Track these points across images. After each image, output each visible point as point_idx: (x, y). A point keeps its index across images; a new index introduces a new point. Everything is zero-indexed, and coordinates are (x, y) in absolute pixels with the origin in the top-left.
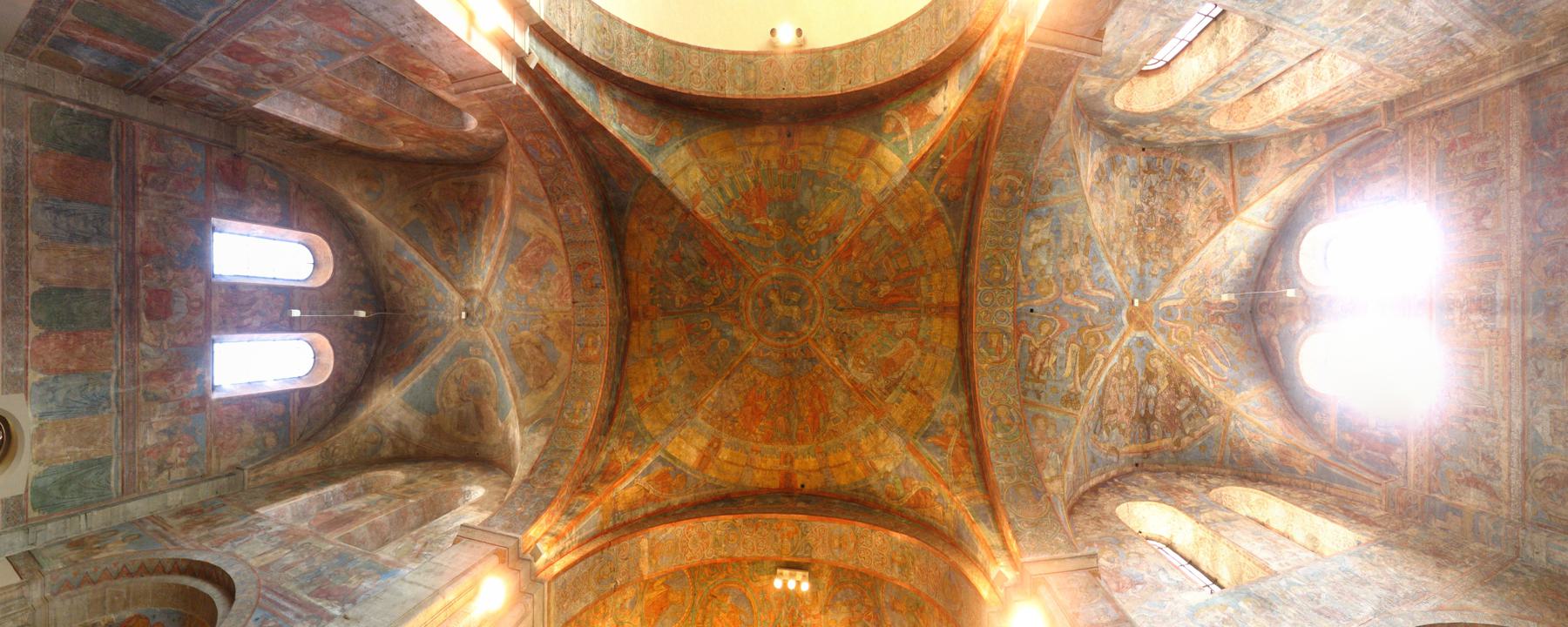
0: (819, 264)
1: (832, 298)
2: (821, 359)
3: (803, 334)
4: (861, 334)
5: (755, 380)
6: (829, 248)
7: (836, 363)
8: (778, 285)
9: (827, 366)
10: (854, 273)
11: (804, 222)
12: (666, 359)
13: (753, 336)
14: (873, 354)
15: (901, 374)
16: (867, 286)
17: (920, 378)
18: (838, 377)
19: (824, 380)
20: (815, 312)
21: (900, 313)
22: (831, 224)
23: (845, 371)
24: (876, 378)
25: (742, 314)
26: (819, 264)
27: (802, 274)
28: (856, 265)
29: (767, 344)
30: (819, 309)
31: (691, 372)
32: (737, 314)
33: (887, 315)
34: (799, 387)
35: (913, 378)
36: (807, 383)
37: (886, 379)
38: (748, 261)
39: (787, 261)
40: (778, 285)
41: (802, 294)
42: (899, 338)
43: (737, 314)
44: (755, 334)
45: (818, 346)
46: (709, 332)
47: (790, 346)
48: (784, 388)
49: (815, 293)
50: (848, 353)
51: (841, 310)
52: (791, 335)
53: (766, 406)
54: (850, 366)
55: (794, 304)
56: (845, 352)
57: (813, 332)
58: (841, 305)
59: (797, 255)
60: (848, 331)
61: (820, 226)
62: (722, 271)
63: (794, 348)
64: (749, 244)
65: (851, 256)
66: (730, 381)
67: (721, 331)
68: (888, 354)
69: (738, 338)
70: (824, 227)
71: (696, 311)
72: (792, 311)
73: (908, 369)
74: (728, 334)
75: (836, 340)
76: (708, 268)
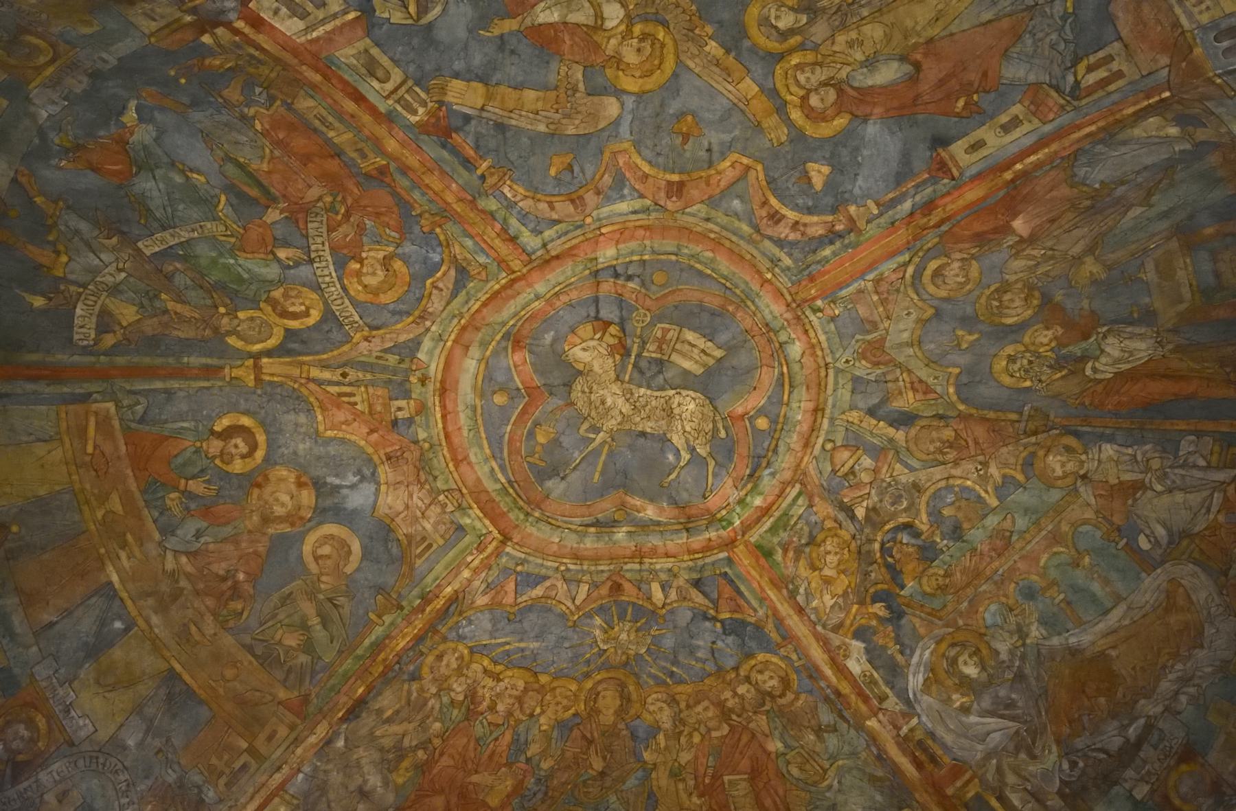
0: (832, 236)
1: (863, 369)
2: (788, 637)
3: (713, 520)
4: (977, 535)
5: (472, 695)
6: (900, 179)
7: (856, 665)
8: (620, 301)
9: (813, 673)
10: (1005, 288)
11: (786, 21)
12: (29, 600)
13: (474, 519)
14: (1022, 633)
15: (1132, 732)
16: (1044, 337)
17: (1213, 757)
18: (860, 727)
19: (790, 721)
20: (779, 424)
21: (1169, 445)
22: (932, 72)
23: (892, 703)
24: (1024, 744)
25: (422, 408)
26: (832, 236)
27: (736, 256)
28: (1018, 264)
29: (540, 552)
30: (799, 408)
31: (172, 676)
32: (403, 408)
33: (1109, 450)
34: (665, 718)
35: (1188, 754)
36: (705, 712)
37: (1067, 751)
38: (492, 204)
39: (676, 189)
40: (620, 301)
41: (731, 349)
42: (1147, 563)
43: (403, 408)
44: (491, 512)
45: (785, 584)
46: (255, 480)
47: (639, 555)
48: (594, 712)
49: (796, 349)
50: (915, 621)
51: (904, 420)
52: (650, 512)
53: (509, 783)
54: (915, 681)
55: (686, 381)
56: (896, 615)
57: (765, 511)
58: (907, 401)
59: (727, 168)
60: (923, 522)
61: (870, 63)
62: (346, 232)
63: (662, 564)
64: (501, 127)
65: (1006, 229)
66: (367, 721)
67: (318, 485)
68: (1084, 638)
69: (403, 529)
70: (889, 73)
71: (180, 373)
72: (669, 413)
73: (1170, 711)
74: (357, 499)
75: (863, 555)
76: (273, 215)
